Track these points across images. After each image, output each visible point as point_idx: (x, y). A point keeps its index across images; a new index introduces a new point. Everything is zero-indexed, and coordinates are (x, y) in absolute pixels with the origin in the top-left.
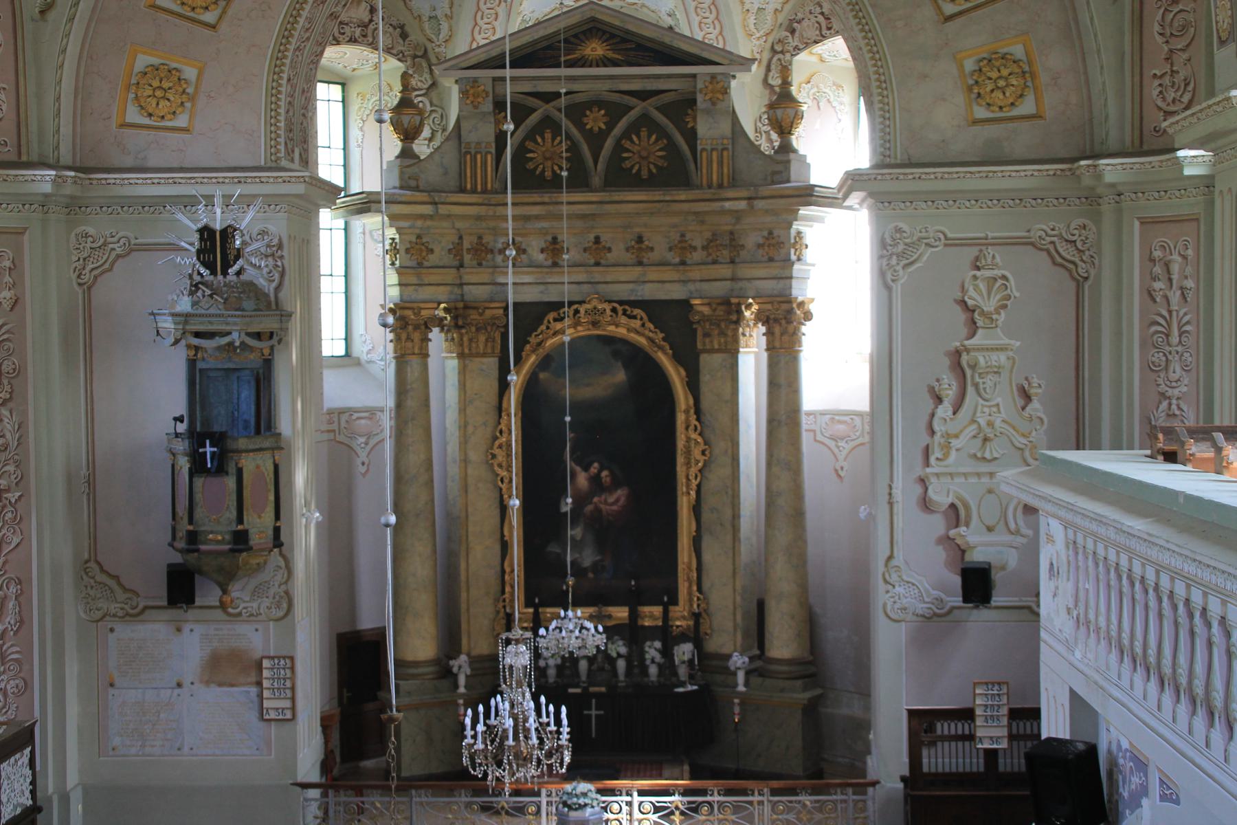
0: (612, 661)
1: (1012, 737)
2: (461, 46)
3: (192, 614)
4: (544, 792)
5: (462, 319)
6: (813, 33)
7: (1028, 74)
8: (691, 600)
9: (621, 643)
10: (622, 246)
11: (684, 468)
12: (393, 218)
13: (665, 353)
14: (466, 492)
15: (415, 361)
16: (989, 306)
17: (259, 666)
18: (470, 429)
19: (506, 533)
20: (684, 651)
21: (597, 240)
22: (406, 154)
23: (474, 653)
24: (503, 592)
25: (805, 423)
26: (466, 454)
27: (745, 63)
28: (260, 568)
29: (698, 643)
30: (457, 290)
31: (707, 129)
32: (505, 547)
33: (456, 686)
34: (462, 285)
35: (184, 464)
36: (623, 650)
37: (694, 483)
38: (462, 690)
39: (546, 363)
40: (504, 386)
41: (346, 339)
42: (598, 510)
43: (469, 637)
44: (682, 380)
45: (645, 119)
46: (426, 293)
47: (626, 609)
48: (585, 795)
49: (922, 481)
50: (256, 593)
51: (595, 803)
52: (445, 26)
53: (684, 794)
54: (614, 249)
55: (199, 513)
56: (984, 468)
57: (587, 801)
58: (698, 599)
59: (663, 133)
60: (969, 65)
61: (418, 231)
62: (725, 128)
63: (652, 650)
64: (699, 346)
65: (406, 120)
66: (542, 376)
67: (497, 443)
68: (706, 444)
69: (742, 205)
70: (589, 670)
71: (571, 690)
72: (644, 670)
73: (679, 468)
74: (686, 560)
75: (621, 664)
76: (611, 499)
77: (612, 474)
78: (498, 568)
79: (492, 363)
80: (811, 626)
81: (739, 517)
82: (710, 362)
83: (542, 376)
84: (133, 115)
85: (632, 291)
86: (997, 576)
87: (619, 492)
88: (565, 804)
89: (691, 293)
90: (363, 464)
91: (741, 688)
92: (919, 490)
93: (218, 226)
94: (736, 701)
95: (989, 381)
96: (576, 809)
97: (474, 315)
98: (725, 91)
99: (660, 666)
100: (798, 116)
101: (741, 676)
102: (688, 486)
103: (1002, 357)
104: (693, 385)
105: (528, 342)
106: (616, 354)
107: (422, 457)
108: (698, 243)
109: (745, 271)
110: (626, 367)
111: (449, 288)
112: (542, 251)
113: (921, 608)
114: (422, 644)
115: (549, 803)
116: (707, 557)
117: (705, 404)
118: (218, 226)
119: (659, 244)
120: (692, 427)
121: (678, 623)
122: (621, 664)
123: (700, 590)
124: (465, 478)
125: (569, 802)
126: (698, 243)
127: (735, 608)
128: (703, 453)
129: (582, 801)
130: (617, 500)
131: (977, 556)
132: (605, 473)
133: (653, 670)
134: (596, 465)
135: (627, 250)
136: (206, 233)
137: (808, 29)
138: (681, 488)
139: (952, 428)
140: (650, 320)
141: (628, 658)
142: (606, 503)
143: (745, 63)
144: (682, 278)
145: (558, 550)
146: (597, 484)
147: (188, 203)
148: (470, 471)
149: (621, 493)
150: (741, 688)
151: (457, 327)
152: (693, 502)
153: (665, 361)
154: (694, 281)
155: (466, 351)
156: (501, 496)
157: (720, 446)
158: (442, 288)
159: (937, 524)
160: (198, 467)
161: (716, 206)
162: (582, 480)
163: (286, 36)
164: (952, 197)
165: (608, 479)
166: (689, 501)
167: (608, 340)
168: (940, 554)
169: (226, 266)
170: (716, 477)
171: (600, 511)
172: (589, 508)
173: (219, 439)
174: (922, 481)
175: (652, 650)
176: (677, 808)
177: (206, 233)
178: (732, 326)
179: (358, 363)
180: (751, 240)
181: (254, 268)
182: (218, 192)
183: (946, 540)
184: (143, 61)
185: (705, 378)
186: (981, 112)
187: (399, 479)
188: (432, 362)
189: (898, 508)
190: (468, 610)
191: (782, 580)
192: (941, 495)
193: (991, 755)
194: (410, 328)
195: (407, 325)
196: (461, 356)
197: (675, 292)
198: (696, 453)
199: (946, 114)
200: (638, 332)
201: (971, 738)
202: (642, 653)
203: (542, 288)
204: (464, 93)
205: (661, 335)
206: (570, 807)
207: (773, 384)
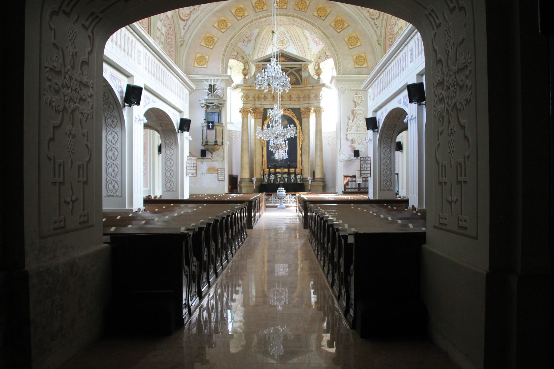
0: (284, 178)
1: (363, 181)
2: (255, 58)
3: (205, 160)
5: (255, 110)
6: (324, 59)
7: (365, 59)
12: (242, 90)
15: (246, 119)
16: (359, 102)
17: (218, 170)
20: (299, 176)
22: (245, 78)
25: (323, 135)
27: (311, 62)
28: (218, 150)
29: (301, 174)
31: (304, 75)
32: (263, 156)
35: (205, 128)
45: (291, 73)
46: (248, 105)
49: (346, 135)
50: (217, 156)
52: (251, 57)
55: (208, 138)
56: (358, 132)
59: (295, 75)
60: (355, 57)
62: (307, 74)
65: (245, 72)
69: (311, 88)
72: (291, 180)
75: (286, 179)
79: (261, 120)
80: (324, 174)
82: (304, 120)
84: (196, 65)
86: (360, 153)
92: (345, 136)
93: (212, 84)
95: (359, 116)
97: (257, 111)
98: (307, 67)
100: (321, 72)
101: (310, 181)
103: (361, 112)
104: (301, 124)
106: (285, 118)
108: (302, 97)
109: (311, 102)
113: (346, 159)
114: (246, 175)
116: (303, 159)
117: (303, 129)
118: (212, 84)
122: (286, 179)
124: (255, 143)
126: (302, 97)
131: (356, 149)
133: (293, 180)
136: (210, 85)
137: (323, 58)
139: (352, 125)
141: (288, 178)
143: (311, 62)
147: (207, 80)
157: (306, 137)
159: (349, 143)
160: (208, 128)
161: (305, 88)
163: (225, 50)
164: (352, 81)
168: (350, 149)
169: (214, 91)
170: (305, 143)
173: (212, 123)
174: (346, 135)
177: (210, 85)
179: (232, 123)
180: (312, 96)
181: (219, 92)
182: (212, 78)
183: (351, 146)
184: (198, 55)
185: (303, 123)
186: (357, 66)
187: (242, 142)
188: (249, 119)
189: (342, 140)
191: (319, 162)
192: (350, 138)
193: (359, 184)
195: (244, 112)
196: (255, 118)
197: (297, 106)
198: (301, 138)
199: (350, 65)
201: (355, 181)
204: (256, 67)
207: (317, 124)
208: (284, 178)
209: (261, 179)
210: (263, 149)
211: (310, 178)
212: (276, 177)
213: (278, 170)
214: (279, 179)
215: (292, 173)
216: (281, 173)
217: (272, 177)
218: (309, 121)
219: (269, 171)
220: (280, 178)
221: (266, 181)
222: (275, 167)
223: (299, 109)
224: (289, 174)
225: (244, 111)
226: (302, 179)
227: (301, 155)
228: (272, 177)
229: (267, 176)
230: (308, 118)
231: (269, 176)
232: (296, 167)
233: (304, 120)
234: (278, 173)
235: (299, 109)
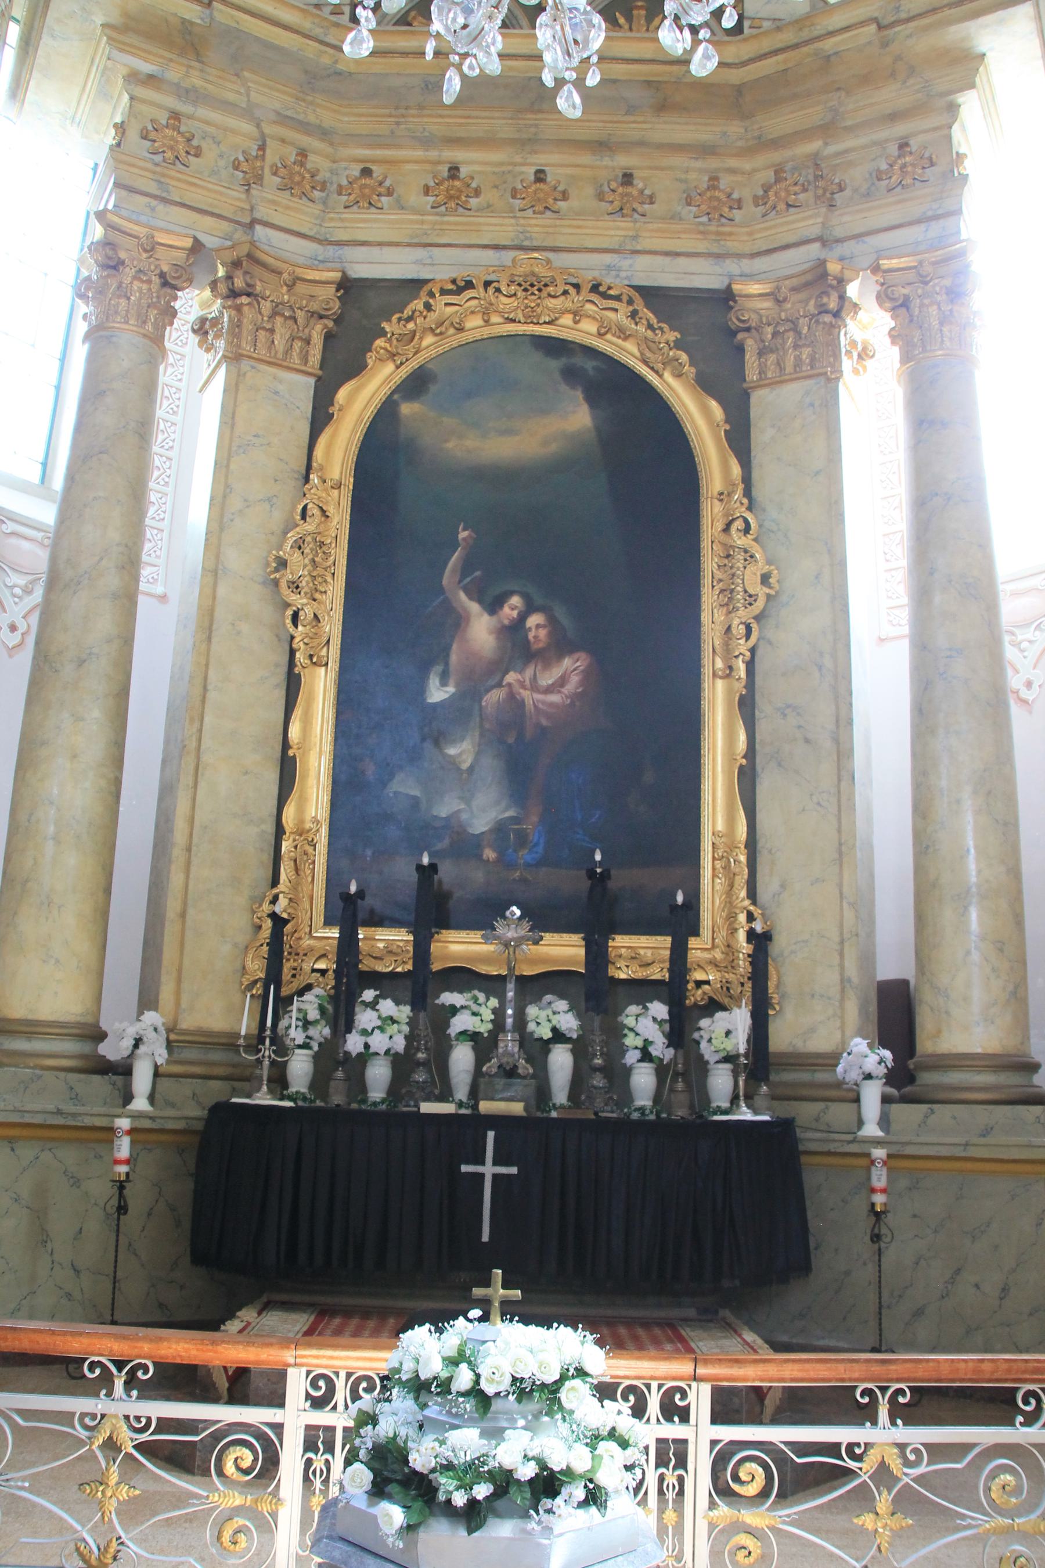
4: (296, 1385)
5: (243, 280)
8: (732, 917)
9: (562, 1005)
10: (590, 191)
11: (720, 616)
13: (678, 375)
14: (209, 639)
15: (128, 340)
18: (235, 503)
19: (295, 732)
20: (728, 1030)
21: (540, 176)
23: (187, 1023)
24: (275, 881)
26: (217, 556)
30: (239, 235)
33: (128, 1097)
34: (254, 222)
36: (569, 1023)
37: (742, 647)
38: (140, 1103)
39: (417, 384)
40: (321, 417)
41: (45, 465)
42: (514, 701)
43: (179, 981)
44: (713, 425)
47: (576, 939)
48: (541, 1395)
51: (611, 1475)
53: (908, 1413)
54: (573, 192)
57: (560, 1450)
58: (751, 917)
61: (171, 102)
63: (646, 1024)
64: (752, 374)
66: (407, 409)
67: (292, 536)
68: (769, 562)
70: (477, 1072)
71: (428, 1108)
72: (618, 1076)
73: (705, 617)
74: (720, 826)
76: (546, 679)
77: (552, 621)
78: (270, 828)
79: (301, 389)
81: (850, 722)
83: (407, 409)
85: (609, 268)
87: (567, 662)
88: (392, 1472)
89: (731, 276)
90: (13, 628)
91: (871, 1129)
94: (879, 1153)
96: (473, 1516)
99: (662, 1071)
101: (872, 1095)
102: (729, 655)
104: (739, 439)
105: (383, 333)
106: (571, 375)
107: (114, 535)
108: (745, 193)
109: (846, 221)
110: (592, 399)
111: (225, 226)
112: (427, 190)
115: (316, 1440)
119: (664, 180)
120: (739, 524)
121: (699, 976)
123: (752, 895)
125: (422, 1457)
127: (842, 942)
128: (765, 579)
129: (516, 1451)
130: (562, 681)
132: (534, 620)
133: (643, 1080)
134: (516, 600)
135: (600, 197)
138: (711, 663)
140: (647, 306)
141: (580, 1049)
142: (534, 687)
144: (715, 250)
145: (416, 792)
146: (515, 644)
148: (222, 591)
149: (571, 669)
150: (871, 1129)
151: (233, 294)
152: (739, 687)
153: (680, 393)
154: (739, 256)
155: (247, 347)
156: (292, 652)
158: (209, 221)
162: (481, 631)
165: (543, 633)
166: (729, 691)
167: (554, 347)
170: (790, 638)
171: (522, 704)
172: (494, 697)
175: (646, 1024)
176: (883, 1474)
178: (827, 318)
185: (761, 435)
190: (183, 915)
194: (129, 273)
196: (234, 357)
197: (702, 275)
198: (751, 579)
200: (624, 334)
202: (615, 1032)
203: (420, 253)
205: (672, 336)
206: (418, 1490)
208: (537, 1051)
209: (228, 1042)
210: (293, 685)
211: (866, 1057)
212: (431, 1035)
213: (458, 946)
214: (462, 1059)
215: (642, 990)
216: (492, 984)
217: (381, 1028)
218: (829, 405)
219: (348, 946)
220: (483, 1045)
221: (300, 1068)
222: (432, 910)
223: (726, 298)
224: (597, 991)
225: (112, 265)
226: (758, 1063)
227: (747, 779)
228: (381, 1028)
229: (310, 1004)
230: (822, 369)
231: (341, 1013)
232: (682, 922)
233: (763, 403)
234: (462, 977)
235: (726, 298)
